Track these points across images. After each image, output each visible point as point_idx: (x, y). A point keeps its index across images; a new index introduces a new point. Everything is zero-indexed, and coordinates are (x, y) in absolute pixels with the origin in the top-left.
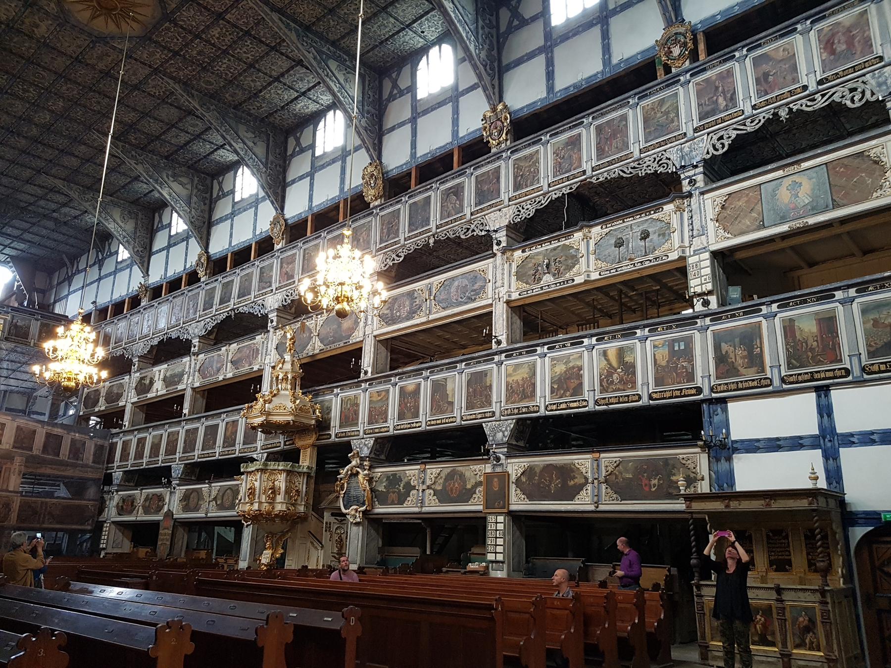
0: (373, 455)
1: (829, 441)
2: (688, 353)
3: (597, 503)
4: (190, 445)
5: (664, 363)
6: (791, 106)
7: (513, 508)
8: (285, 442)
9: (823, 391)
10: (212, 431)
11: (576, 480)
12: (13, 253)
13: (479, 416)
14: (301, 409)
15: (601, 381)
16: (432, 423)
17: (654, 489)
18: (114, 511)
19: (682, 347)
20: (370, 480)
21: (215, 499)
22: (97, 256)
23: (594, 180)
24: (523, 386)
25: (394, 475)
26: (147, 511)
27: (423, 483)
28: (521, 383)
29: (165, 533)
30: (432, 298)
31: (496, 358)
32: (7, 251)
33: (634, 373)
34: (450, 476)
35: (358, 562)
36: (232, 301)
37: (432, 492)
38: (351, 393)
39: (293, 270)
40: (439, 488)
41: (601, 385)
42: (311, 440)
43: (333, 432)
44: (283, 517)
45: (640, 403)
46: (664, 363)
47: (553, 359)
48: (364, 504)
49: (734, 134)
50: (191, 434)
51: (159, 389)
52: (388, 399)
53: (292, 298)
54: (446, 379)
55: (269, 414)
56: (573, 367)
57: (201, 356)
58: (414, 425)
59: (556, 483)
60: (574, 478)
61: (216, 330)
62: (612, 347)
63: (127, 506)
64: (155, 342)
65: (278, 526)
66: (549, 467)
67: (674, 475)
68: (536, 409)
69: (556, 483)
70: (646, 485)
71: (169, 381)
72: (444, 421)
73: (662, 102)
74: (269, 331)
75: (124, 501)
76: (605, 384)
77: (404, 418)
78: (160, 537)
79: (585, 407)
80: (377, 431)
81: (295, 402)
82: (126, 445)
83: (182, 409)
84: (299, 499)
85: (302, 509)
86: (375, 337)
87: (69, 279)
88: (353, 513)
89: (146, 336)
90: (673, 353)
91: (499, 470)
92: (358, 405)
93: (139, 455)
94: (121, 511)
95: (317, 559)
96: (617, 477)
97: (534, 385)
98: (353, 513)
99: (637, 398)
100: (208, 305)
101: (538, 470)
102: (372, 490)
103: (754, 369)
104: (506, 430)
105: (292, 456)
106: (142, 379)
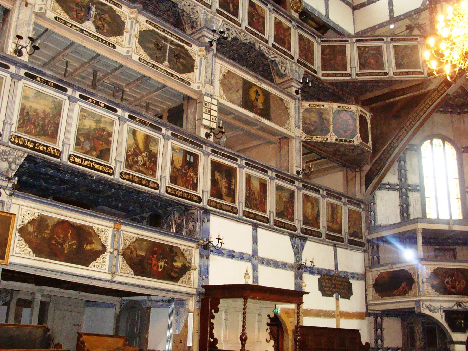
1: (254, 258)
3: (113, 274)
5: (178, 166)
6: (261, 45)
11: (93, 246)
17: (160, 270)
19: (192, 161)
24: (44, 119)
28: (41, 115)
33: (155, 163)
41: (127, 160)
45: (158, 191)
46: (178, 166)
47: (82, 110)
49: (235, 35)
56: (103, 130)
60: (91, 243)
62: (143, 130)
66: (64, 224)
67: (176, 261)
68: (56, 153)
69: (70, 244)
70: (155, 265)
76: (130, 161)
79: (110, 174)
96: (132, 252)
99: (155, 186)
101: (50, 224)
103: (230, 199)
104: (14, 161)
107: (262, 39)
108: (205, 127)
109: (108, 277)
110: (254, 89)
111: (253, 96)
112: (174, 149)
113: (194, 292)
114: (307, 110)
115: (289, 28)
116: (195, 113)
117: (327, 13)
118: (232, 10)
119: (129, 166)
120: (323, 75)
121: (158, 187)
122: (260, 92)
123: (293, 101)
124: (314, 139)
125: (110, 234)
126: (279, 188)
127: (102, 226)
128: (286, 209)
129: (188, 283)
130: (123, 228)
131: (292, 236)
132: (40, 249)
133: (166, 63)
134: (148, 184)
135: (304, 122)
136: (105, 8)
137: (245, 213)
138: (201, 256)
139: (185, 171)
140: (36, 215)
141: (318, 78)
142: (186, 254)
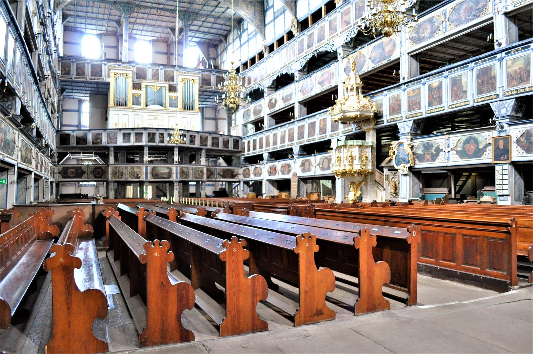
0: (412, 132)
4: (301, 135)
7: (514, 159)
8: (356, 128)
10: (313, 125)
12: (198, 40)
13: (487, 99)
14: (364, 107)
16: (453, 106)
18: (267, 174)
20: (412, 148)
21: (319, 164)
22: (238, 33)
24: (520, 73)
25: (428, 143)
26: (283, 173)
27: (448, 147)
28: (518, 71)
29: (294, 185)
30: (447, 20)
31: (498, 56)
32: (194, 39)
34: (467, 141)
35: (408, 198)
36: (314, 45)
37: (455, 152)
38: (394, 93)
39: (349, 19)
40: (459, 149)
42: (372, 126)
43: (385, 119)
44: (360, 173)
48: (408, 162)
50: (301, 128)
51: (280, 106)
52: (420, 94)
53: (350, 37)
54: (461, 76)
55: (344, 112)
57: (301, 82)
58: (440, 109)
61: (307, 65)
63: (272, 171)
64: (275, 78)
65: (357, 179)
71: (285, 100)
72: (461, 105)
74: (338, 61)
75: (271, 168)
77: (432, 105)
78: (292, 187)
80: (414, 115)
81: (359, 103)
82: (267, 138)
83: (294, 115)
84: (368, 162)
85: (370, 168)
86: (408, 53)
87: (225, 49)
88: (403, 168)
89: (269, 75)
91: (503, 134)
92: (400, 100)
93: (275, 143)
94: (270, 173)
95: (382, 196)
98: (403, 169)
100: (301, 51)
102: (413, 154)
104: (509, 106)
105: (361, 136)
106: (271, 100)
140: (524, 131)
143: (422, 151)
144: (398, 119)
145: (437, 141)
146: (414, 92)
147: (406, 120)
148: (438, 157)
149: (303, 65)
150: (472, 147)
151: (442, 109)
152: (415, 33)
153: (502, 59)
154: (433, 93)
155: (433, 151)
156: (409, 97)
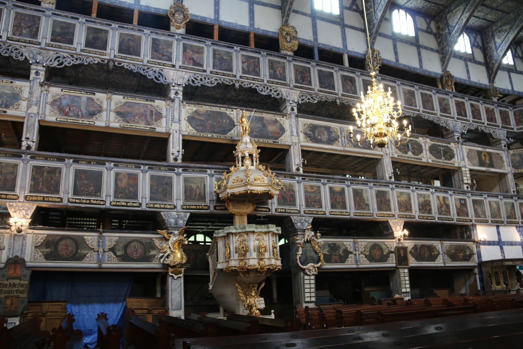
1: (500, 243)
2: (465, 205)
3: (444, 263)
5: (459, 207)
7: (411, 265)
9: (498, 227)
15: (438, 209)
16: (357, 214)
23: (423, 116)
24: (406, 204)
25: (334, 244)
28: (405, 202)
37: (364, 257)
40: (368, 253)
47: (418, 194)
49: (468, 127)
52: (320, 192)
53: (202, 83)
54: (362, 190)
56: (427, 200)
58: (345, 214)
59: (427, 254)
60: (434, 251)
62: (441, 195)
66: (423, 246)
73: (444, 99)
86: (301, 146)
90: (461, 204)
91: (400, 245)
92: (294, 191)
97: (411, 205)
101: (419, 247)
107: (481, 123)
108: (466, 184)
109: (442, 265)
110: (483, 154)
111: (483, 158)
112: (455, 200)
113: (477, 265)
114: (513, 155)
115: (493, 109)
116: (459, 177)
117: (512, 88)
118: (463, 114)
119: (440, 214)
120: (517, 129)
121: (453, 220)
122: (486, 154)
123: (503, 152)
124: (520, 171)
125: (440, 246)
126: (506, 203)
127: (437, 244)
128: (511, 213)
129: (473, 260)
130: (444, 242)
131: (516, 227)
132: (419, 258)
133: (443, 158)
134: (448, 219)
135: (512, 162)
136: (413, 142)
137: (492, 222)
138: (476, 247)
139: (462, 209)
141: (515, 132)
142: (470, 247)
143: (328, 251)
144: (293, 211)
145: (345, 243)
146: (312, 188)
147: (305, 215)
148: (348, 259)
149: (66, 63)
150: (378, 253)
151: (347, 214)
152: (310, 131)
153: (392, 189)
154: (335, 196)
155: (341, 252)
156: (306, 192)
